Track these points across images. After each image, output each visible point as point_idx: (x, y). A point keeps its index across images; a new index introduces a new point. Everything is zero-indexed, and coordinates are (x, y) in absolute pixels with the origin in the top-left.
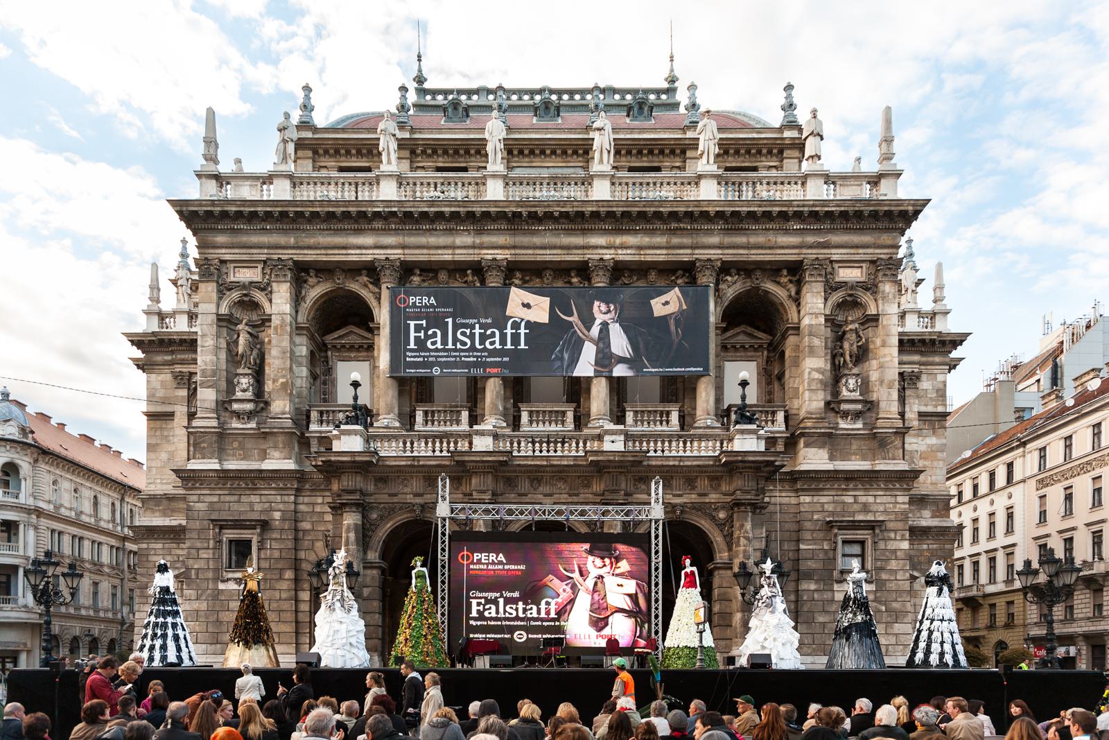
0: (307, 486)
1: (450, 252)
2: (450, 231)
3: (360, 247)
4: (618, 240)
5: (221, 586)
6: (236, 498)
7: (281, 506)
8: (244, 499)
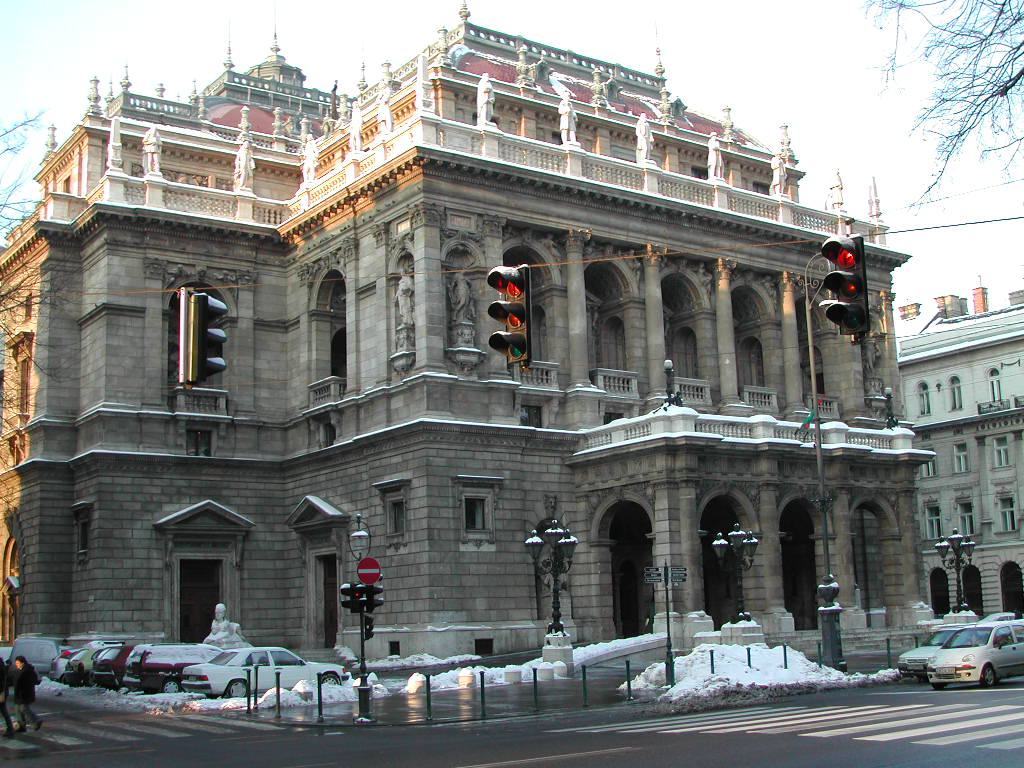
0: (528, 446)
1: (625, 233)
2: (624, 215)
3: (559, 217)
4: (738, 245)
5: (463, 548)
6: (468, 454)
7: (510, 465)
8: (478, 455)
